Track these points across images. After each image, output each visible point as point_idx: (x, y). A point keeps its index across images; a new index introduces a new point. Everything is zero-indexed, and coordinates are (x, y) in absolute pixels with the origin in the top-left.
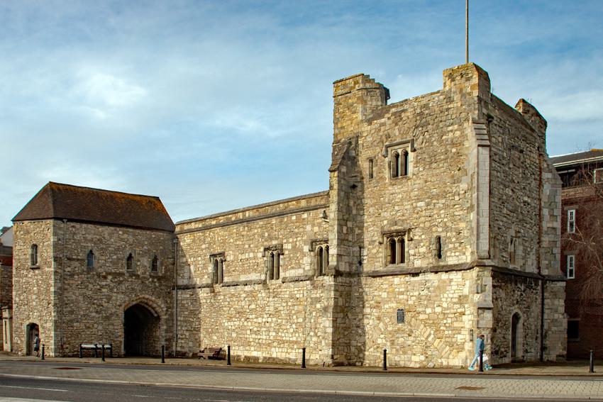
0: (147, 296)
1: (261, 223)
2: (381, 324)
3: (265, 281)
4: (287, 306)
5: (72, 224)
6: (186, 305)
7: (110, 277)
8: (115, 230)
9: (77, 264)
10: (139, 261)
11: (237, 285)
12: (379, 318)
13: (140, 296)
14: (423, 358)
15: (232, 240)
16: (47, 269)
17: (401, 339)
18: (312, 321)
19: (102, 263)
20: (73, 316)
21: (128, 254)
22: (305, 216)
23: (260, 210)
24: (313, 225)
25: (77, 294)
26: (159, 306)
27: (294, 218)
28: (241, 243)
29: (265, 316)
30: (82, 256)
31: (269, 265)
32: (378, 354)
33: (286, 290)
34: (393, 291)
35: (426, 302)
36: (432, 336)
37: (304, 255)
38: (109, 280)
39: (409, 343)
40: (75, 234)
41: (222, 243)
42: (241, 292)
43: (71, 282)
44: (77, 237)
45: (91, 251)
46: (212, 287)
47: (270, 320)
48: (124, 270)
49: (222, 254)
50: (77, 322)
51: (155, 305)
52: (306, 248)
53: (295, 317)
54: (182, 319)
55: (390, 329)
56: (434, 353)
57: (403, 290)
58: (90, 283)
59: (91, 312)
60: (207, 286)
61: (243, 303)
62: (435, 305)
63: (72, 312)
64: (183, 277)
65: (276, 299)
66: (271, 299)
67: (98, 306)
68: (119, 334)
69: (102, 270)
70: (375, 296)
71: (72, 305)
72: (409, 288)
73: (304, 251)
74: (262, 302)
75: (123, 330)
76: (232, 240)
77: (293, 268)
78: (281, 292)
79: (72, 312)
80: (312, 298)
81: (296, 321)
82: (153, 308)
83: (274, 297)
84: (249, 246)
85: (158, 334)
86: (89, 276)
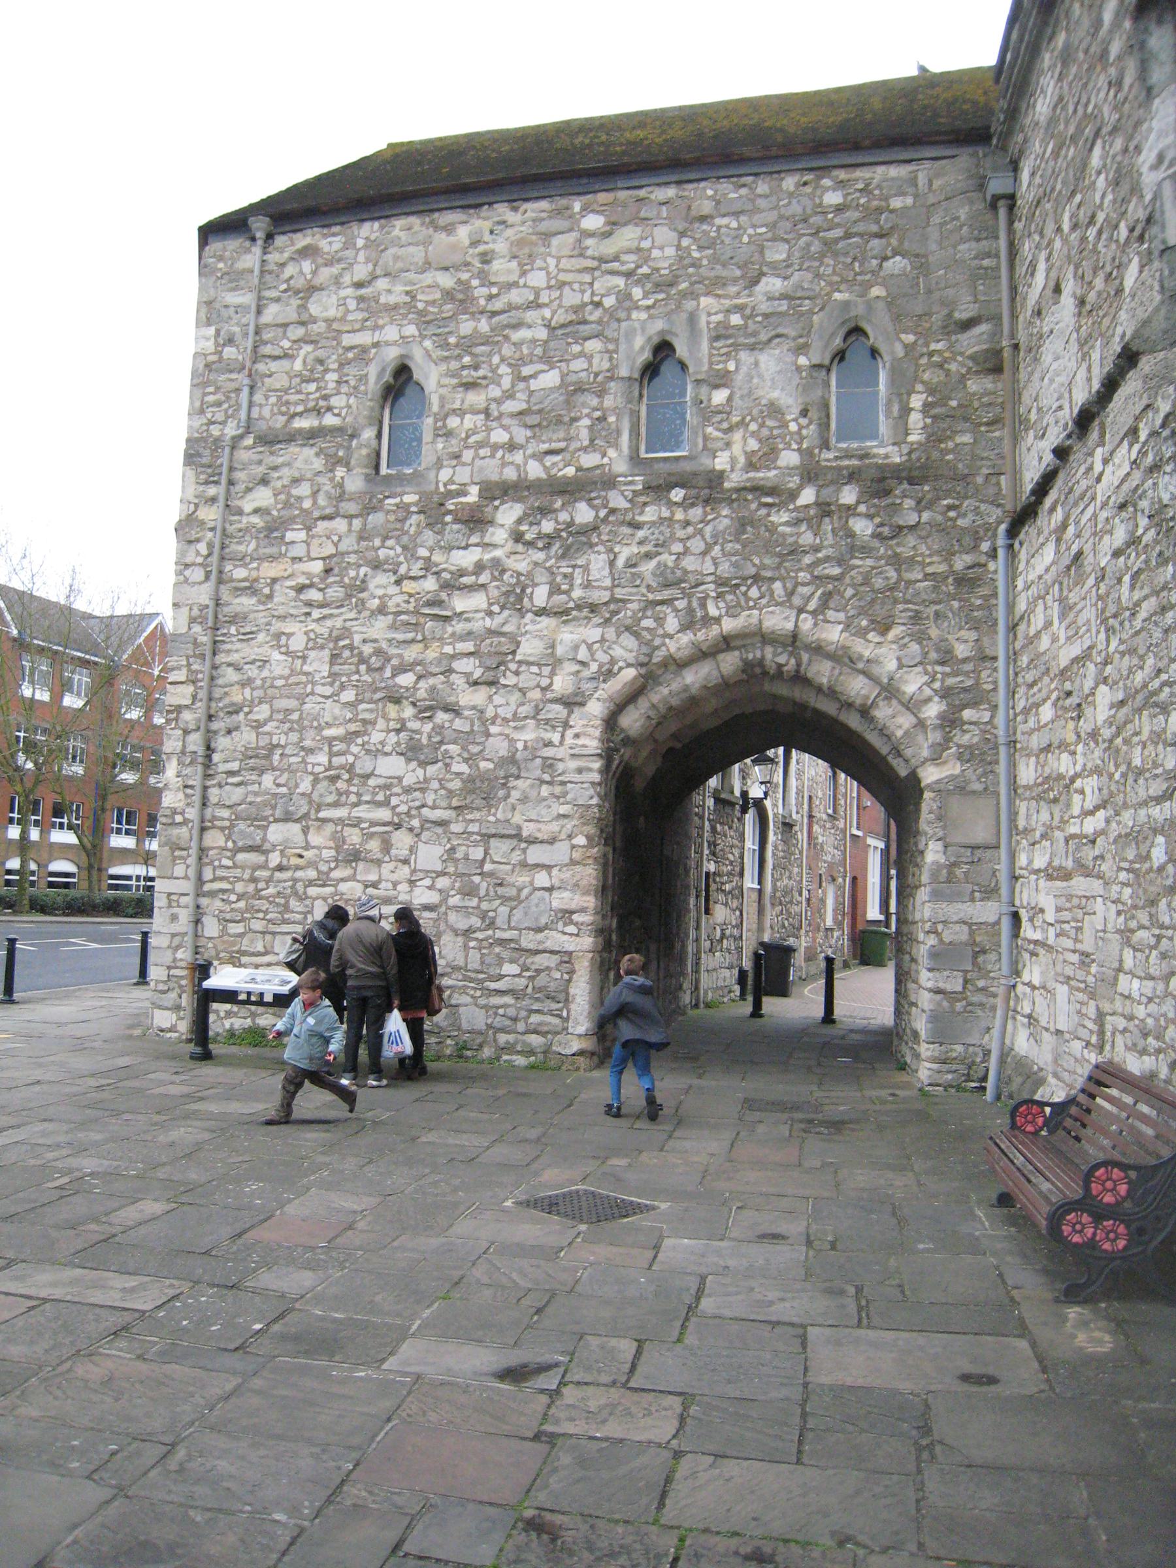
0: (778, 621)
5: (302, 240)
8: (558, 213)
9: (306, 459)
10: (721, 380)
13: (729, 625)
19: (472, 439)
20: (268, 780)
21: (639, 350)
25: (297, 643)
26: (890, 691)
30: (349, 405)
38: (499, 535)
40: (312, 289)
43: (270, 570)
44: (323, 307)
50: (287, 818)
51: (857, 687)
58: (377, 566)
59: (376, 753)
63: (260, 759)
67: (426, 712)
68: (561, 900)
75: (589, 874)
79: (260, 759)
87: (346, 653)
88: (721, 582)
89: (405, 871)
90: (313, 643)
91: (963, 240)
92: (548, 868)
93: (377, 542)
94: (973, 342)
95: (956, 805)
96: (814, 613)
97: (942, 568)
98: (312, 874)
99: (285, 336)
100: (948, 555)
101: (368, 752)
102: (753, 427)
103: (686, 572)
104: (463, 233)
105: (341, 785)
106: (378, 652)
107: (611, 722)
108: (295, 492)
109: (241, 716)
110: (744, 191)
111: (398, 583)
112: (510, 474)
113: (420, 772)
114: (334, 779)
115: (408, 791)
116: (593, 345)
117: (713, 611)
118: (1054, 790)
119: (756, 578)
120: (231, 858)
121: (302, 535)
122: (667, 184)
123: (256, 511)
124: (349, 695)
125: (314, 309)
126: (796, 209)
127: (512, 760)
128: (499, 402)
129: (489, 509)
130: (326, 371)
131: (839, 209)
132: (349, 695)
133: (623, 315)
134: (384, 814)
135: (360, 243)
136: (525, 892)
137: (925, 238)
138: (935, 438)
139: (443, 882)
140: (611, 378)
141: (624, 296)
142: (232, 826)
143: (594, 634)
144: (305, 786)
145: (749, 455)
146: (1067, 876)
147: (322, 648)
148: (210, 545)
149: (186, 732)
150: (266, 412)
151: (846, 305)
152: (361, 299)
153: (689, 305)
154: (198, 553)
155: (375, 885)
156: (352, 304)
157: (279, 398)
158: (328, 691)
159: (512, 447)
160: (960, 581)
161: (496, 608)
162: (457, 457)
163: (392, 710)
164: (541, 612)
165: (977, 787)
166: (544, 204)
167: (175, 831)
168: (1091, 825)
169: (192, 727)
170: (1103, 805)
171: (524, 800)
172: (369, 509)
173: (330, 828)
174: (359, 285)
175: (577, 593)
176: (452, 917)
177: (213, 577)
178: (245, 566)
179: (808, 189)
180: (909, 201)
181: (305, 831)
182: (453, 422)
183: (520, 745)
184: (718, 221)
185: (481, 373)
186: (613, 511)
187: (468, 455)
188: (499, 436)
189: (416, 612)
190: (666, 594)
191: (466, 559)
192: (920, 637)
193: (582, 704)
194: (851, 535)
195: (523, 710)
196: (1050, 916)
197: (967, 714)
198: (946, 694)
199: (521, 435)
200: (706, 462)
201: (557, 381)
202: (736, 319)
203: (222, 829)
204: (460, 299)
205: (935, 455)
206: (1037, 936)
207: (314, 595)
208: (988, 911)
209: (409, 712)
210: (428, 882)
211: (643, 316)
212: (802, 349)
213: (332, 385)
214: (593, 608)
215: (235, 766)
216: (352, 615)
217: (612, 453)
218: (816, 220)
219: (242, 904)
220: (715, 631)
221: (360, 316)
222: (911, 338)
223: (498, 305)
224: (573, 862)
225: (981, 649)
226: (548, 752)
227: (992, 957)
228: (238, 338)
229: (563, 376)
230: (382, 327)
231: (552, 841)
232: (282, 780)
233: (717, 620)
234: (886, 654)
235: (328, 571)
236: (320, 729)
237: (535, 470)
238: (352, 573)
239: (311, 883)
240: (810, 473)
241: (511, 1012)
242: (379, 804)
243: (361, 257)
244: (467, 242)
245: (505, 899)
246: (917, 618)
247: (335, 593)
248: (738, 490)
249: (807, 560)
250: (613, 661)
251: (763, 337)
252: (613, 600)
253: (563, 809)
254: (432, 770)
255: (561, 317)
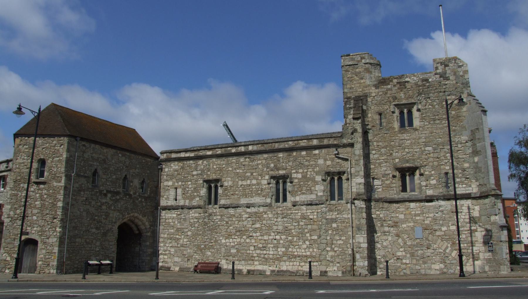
0: (136, 215)
1: (265, 156)
2: (400, 240)
3: (271, 204)
4: (299, 225)
5: (83, 143)
6: (172, 224)
7: (109, 195)
11: (237, 207)
12: (398, 236)
14: (442, 266)
15: (230, 169)
16: (55, 184)
17: (420, 252)
18: (328, 238)
20: (76, 232)
22: (317, 152)
23: (265, 145)
24: (325, 160)
25: (82, 210)
27: (304, 153)
28: (241, 171)
29: (273, 234)
30: (89, 173)
31: (274, 190)
32: (398, 265)
33: (297, 212)
34: (410, 214)
35: (441, 222)
36: (449, 248)
37: (317, 183)
38: (108, 198)
39: (429, 254)
41: (218, 171)
42: (243, 213)
44: (86, 156)
45: (96, 170)
46: (205, 208)
47: (278, 237)
48: (121, 190)
49: (217, 181)
50: (80, 237)
51: (140, 223)
52: (319, 178)
53: (308, 235)
54: (166, 236)
55: (409, 243)
56: (452, 262)
57: (419, 212)
58: (93, 200)
59: (92, 228)
60: (199, 207)
61: (245, 223)
62: (450, 225)
64: (168, 199)
65: (285, 219)
66: (279, 219)
68: (113, 250)
70: (393, 217)
71: (76, 220)
72: (425, 211)
73: (316, 180)
74: (269, 222)
76: (230, 169)
77: (303, 193)
78: (291, 213)
80: (327, 219)
81: (309, 238)
82: (137, 226)
83: (283, 218)
84: (252, 174)
85: (137, 249)
86: (93, 193)
112: (109, 189)
124: (88, 219)
132: (88, 219)
141: (123, 168)
198: (150, 225)
204: (104, 160)
209: (96, 222)
234: (145, 219)
237: (112, 189)
247: (87, 203)
254: (99, 231)
255: (116, 168)
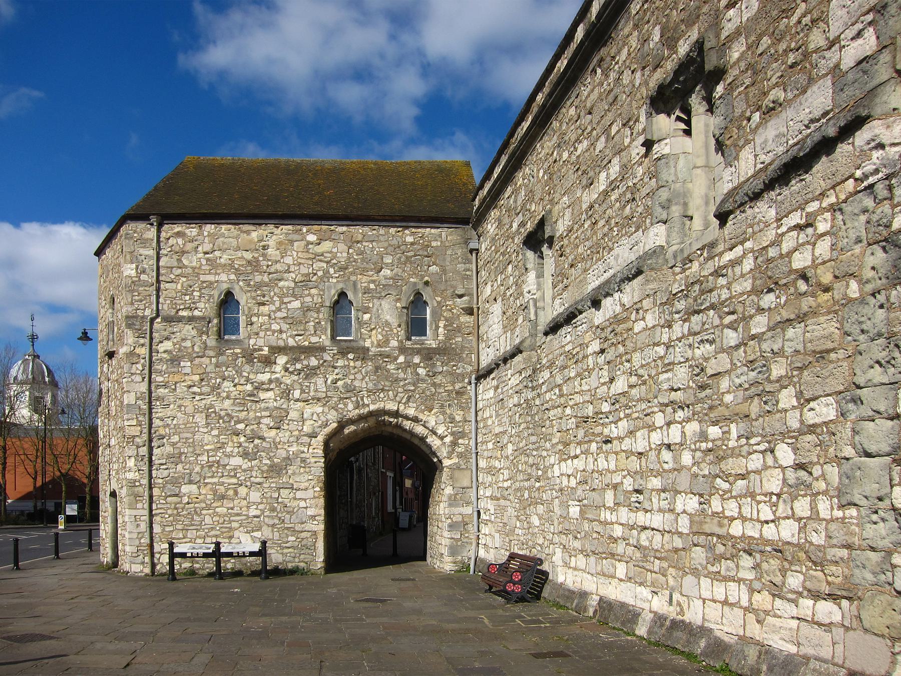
0: (391, 406)
5: (177, 228)
7: (282, 360)
9: (188, 330)
10: (366, 310)
13: (372, 407)
19: (261, 326)
20: (180, 467)
21: (333, 294)
25: (190, 409)
30: (206, 308)
40: (184, 252)
43: (173, 379)
48: (325, 339)
50: (191, 482)
51: (419, 430)
59: (229, 456)
63: (176, 458)
67: (251, 439)
68: (310, 512)
69: (260, 342)
71: (175, 439)
75: (322, 501)
79: (176, 458)
86: (222, 359)
87: (213, 415)
88: (369, 391)
89: (244, 503)
90: (197, 410)
91: (459, 263)
92: (305, 500)
93: (224, 369)
94: (462, 302)
95: (457, 474)
96: (404, 404)
97: (451, 388)
98: (204, 505)
99: (171, 272)
100: (453, 384)
101: (226, 456)
102: (379, 330)
103: (355, 387)
104: (254, 235)
105: (213, 469)
106: (228, 415)
107: (326, 444)
108: (183, 344)
109: (165, 440)
110: (374, 232)
111: (235, 386)
113: (249, 464)
114: (210, 467)
115: (245, 471)
116: (313, 291)
117: (366, 402)
118: (491, 471)
119: (383, 390)
120: (165, 500)
121: (189, 364)
122: (343, 225)
123: (165, 352)
125: (185, 262)
126: (395, 242)
127: (288, 458)
128: (274, 312)
129: (273, 358)
130: (194, 291)
131: (412, 244)
133: (326, 280)
134: (234, 481)
135: (206, 234)
136: (296, 510)
137: (444, 260)
138: (448, 338)
139: (261, 507)
140: (322, 306)
142: (164, 487)
143: (320, 410)
144: (198, 469)
145: (379, 341)
146: (498, 499)
147: (202, 412)
148: (144, 366)
149: (138, 447)
150: (165, 307)
151: (415, 283)
152: (208, 260)
153: (353, 278)
154: (137, 369)
155: (232, 509)
156: (204, 262)
157: (171, 301)
158: (205, 430)
159: (281, 331)
160: (457, 393)
161: (278, 398)
162: (257, 334)
163: (235, 438)
164: (297, 400)
165: (464, 467)
166: (290, 227)
167: (136, 489)
168: (506, 484)
169: (141, 444)
170: (510, 479)
171: (294, 474)
172: (220, 353)
173: (209, 486)
174: (206, 253)
175: (312, 394)
176: (266, 520)
177: (146, 379)
178: (162, 376)
179: (400, 234)
180: (439, 243)
181: (199, 488)
182: (254, 319)
183: (291, 453)
184: (364, 244)
185: (266, 299)
186: (325, 361)
187: (262, 334)
188: (275, 327)
189: (244, 399)
190: (348, 395)
191: (265, 377)
192: (444, 413)
193: (316, 437)
194: (418, 374)
195: (291, 439)
196: (492, 512)
197: (460, 441)
198: (452, 434)
199: (285, 327)
200: (362, 343)
201: (300, 306)
202: (372, 286)
203: (159, 488)
204: (254, 265)
205: (448, 344)
206: (488, 518)
207: (195, 389)
208: (468, 510)
209: (242, 439)
210: (255, 507)
211: (335, 280)
212: (399, 300)
213: (197, 298)
214: (319, 400)
215: (164, 461)
216: (215, 399)
217: (323, 337)
218: (403, 247)
219: (171, 518)
220: (367, 410)
221: (208, 268)
222: (439, 299)
223: (272, 270)
224: (315, 497)
225: (465, 418)
226: (303, 455)
227: (470, 526)
228: (148, 271)
229: (302, 304)
230: (219, 274)
231: (306, 489)
232: (187, 467)
233: (368, 406)
235: (202, 380)
236: (202, 446)
237: (291, 342)
238: (213, 381)
239: (203, 509)
240: (402, 350)
241: (293, 555)
242: (232, 477)
243: (206, 240)
244: (256, 240)
245: (288, 512)
246: (442, 406)
247: (206, 389)
248: (374, 355)
249: (402, 383)
250: (327, 421)
251: (383, 295)
252: (327, 396)
253: (310, 477)
